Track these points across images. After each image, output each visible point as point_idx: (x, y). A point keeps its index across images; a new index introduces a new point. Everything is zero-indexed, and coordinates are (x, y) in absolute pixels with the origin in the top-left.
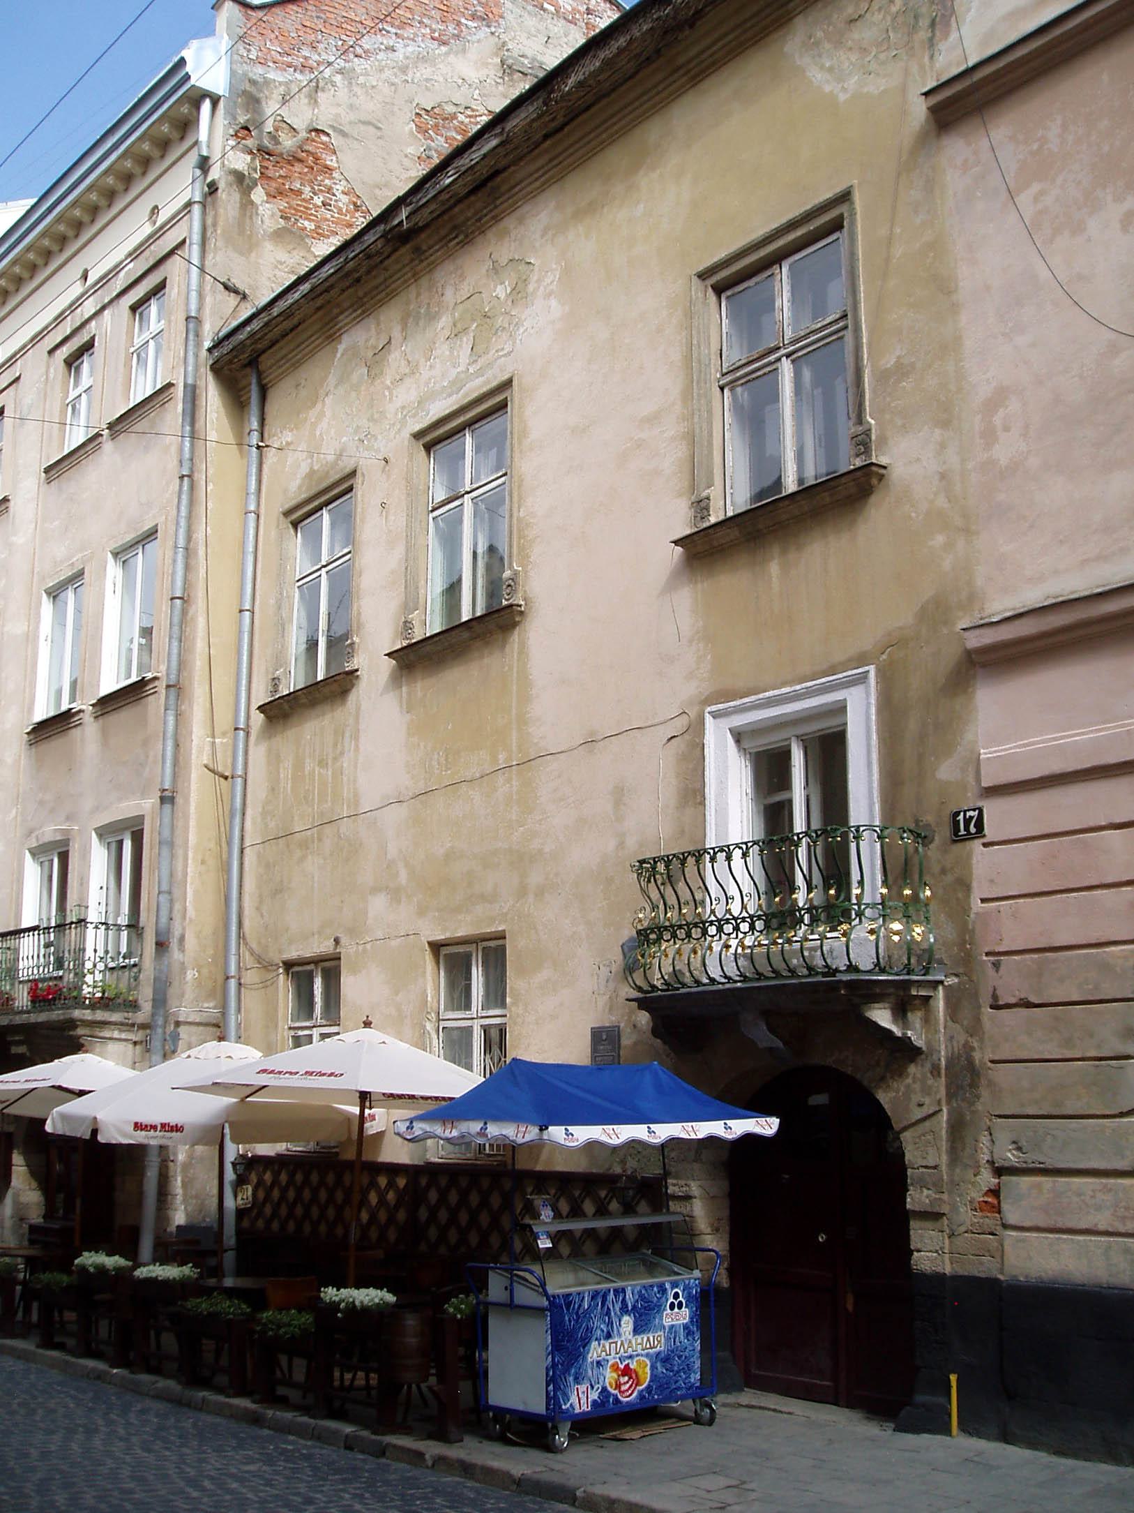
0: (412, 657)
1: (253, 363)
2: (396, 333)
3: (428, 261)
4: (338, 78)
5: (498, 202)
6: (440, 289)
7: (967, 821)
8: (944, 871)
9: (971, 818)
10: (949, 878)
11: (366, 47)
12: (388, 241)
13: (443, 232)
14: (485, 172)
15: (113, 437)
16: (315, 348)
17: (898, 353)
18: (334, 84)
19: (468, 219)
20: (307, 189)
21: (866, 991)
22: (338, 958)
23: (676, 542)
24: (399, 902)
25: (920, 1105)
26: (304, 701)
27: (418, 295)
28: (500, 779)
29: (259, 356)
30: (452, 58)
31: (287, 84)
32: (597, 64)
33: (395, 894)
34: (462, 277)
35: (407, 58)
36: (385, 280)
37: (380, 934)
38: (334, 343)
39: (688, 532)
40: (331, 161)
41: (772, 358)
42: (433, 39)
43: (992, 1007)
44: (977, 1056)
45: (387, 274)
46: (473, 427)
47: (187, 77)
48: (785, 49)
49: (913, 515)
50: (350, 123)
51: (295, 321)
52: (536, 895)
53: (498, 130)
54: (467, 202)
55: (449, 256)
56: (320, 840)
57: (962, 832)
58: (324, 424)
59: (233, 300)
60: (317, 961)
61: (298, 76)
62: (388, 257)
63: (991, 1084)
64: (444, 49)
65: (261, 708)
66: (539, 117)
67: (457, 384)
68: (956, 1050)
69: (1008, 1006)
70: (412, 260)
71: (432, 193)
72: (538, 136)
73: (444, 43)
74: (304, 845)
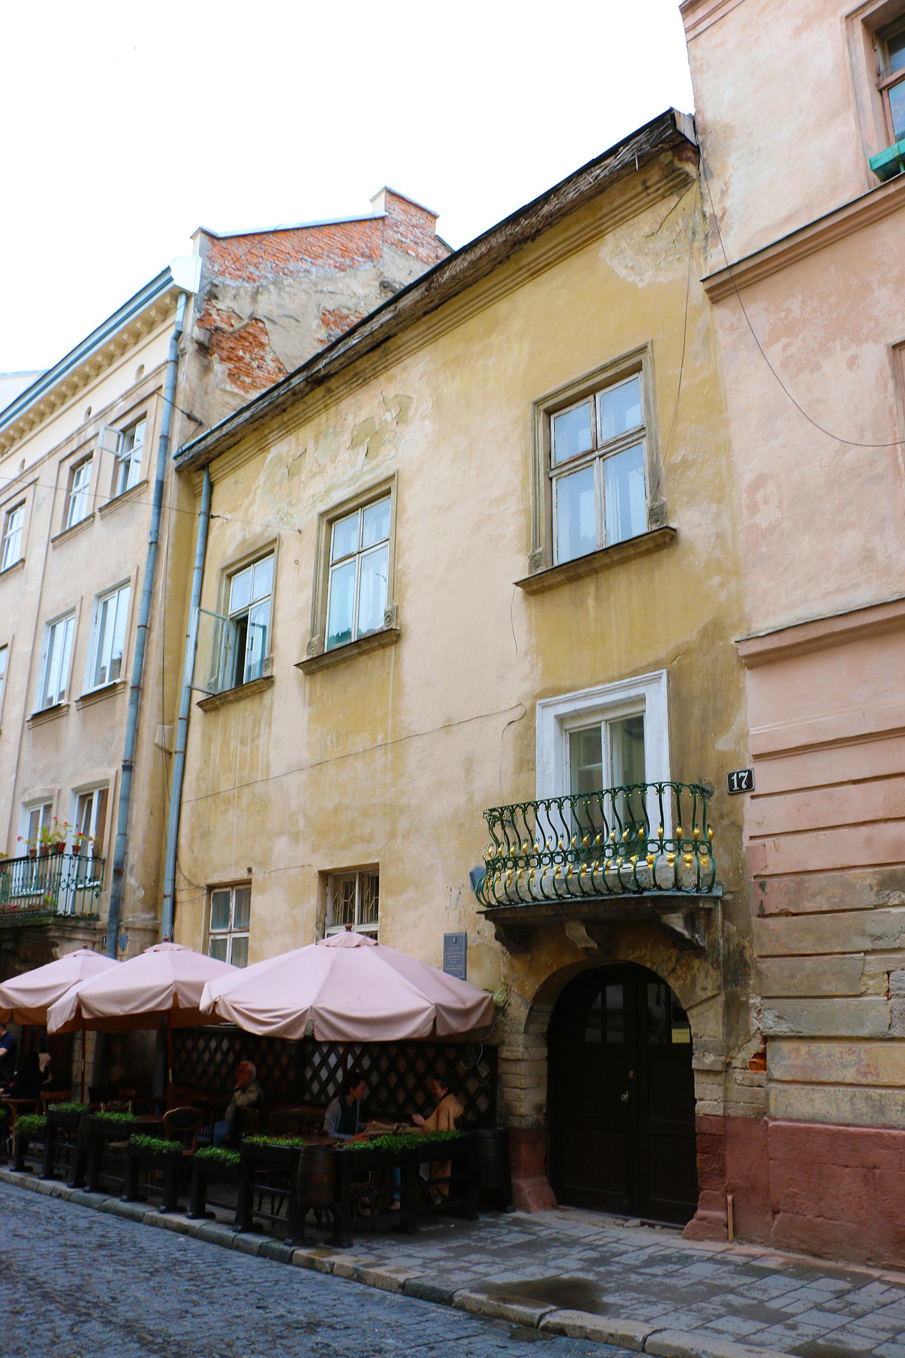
0: (314, 667)
1: (205, 467)
2: (311, 446)
3: (336, 397)
4: (272, 287)
5: (388, 357)
6: (343, 417)
7: (740, 781)
8: (721, 817)
9: (743, 778)
10: (726, 822)
11: (291, 268)
12: (308, 383)
13: (347, 377)
14: (380, 336)
15: (102, 518)
17: (683, 452)
18: (269, 291)
19: (366, 368)
20: (247, 356)
21: (668, 904)
22: (249, 882)
23: (517, 584)
24: (297, 841)
25: (705, 989)
26: (232, 698)
27: (328, 419)
29: (210, 462)
30: (347, 280)
31: (238, 288)
32: (466, 264)
33: (295, 837)
34: (360, 408)
35: (318, 278)
36: (304, 410)
37: (282, 866)
38: (264, 454)
39: (526, 576)
40: (264, 340)
41: (589, 458)
42: (336, 267)
43: (759, 916)
44: (747, 953)
46: (364, 508)
47: (171, 280)
48: (599, 255)
49: (697, 563)
50: (279, 316)
51: (238, 438)
52: (404, 837)
53: (392, 308)
54: (366, 357)
55: (351, 392)
56: (239, 797)
57: (736, 788)
58: (254, 508)
59: (193, 426)
60: (232, 885)
61: (245, 284)
62: (307, 394)
63: (759, 973)
64: (342, 274)
65: (200, 704)
66: (423, 299)
67: (354, 478)
68: (731, 948)
69: (771, 915)
70: (324, 396)
71: (342, 350)
72: (420, 313)
73: (343, 270)
74: (227, 801)
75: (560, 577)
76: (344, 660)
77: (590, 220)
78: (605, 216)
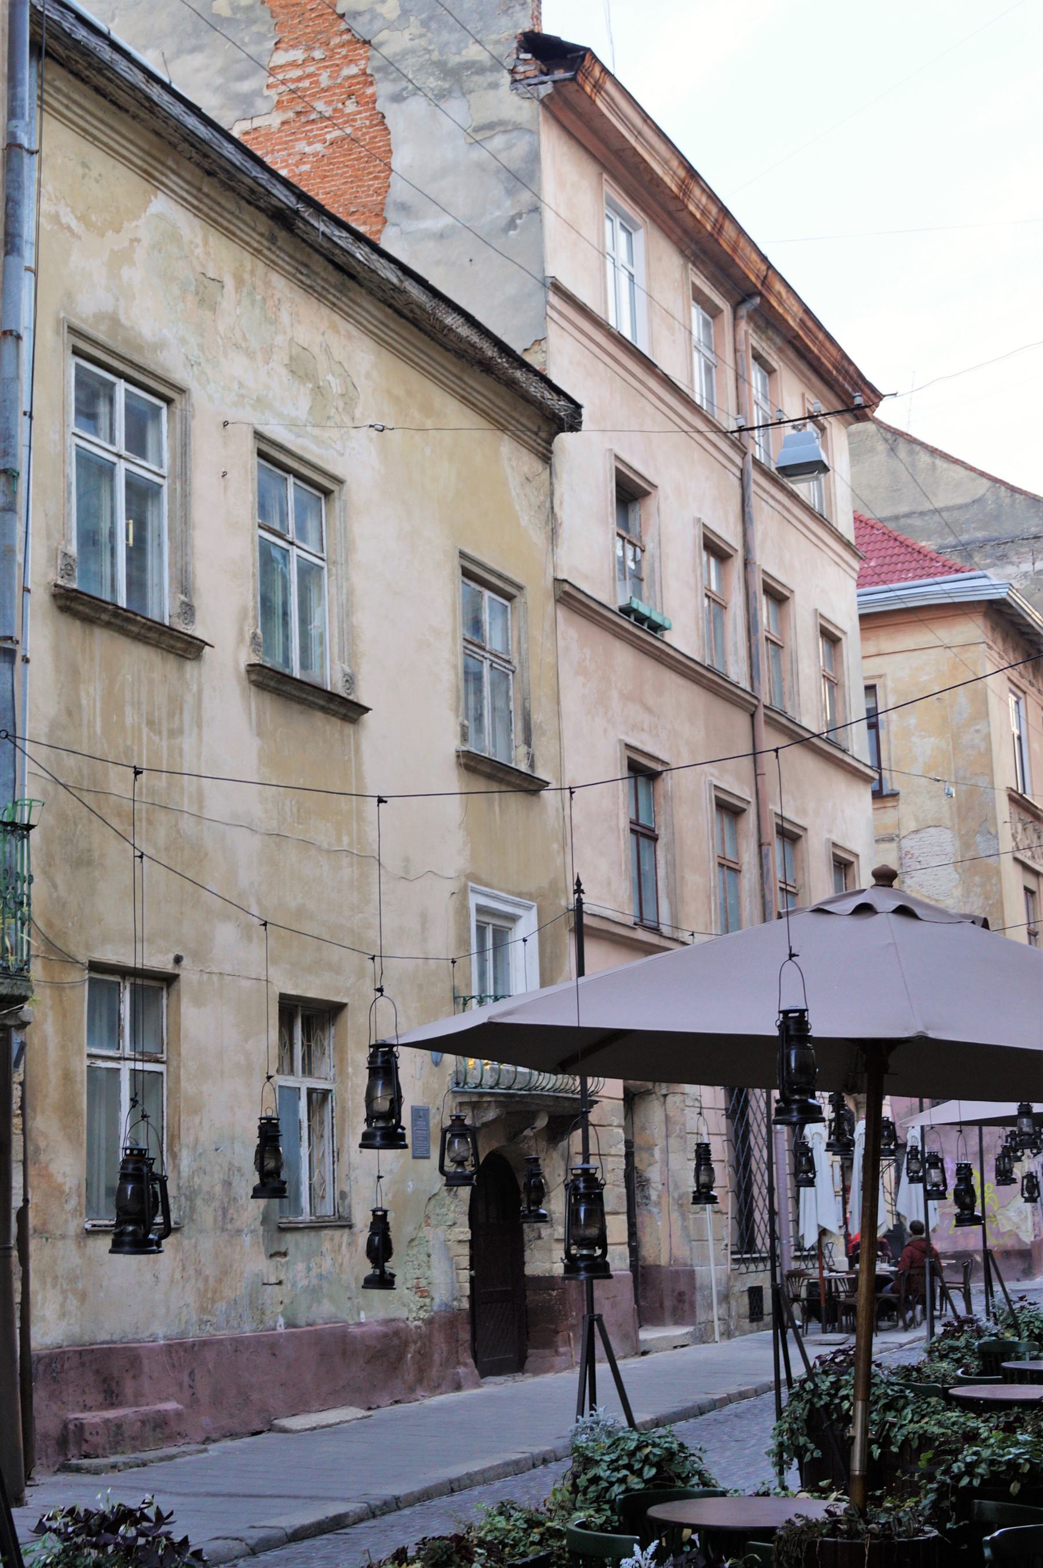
13: (298, 256)
16: (124, 157)
24: (250, 939)
28: (345, 861)
37: (228, 968)
45: (237, 212)
75: (488, 770)
76: (301, 701)
77: (507, 409)
78: (518, 421)
